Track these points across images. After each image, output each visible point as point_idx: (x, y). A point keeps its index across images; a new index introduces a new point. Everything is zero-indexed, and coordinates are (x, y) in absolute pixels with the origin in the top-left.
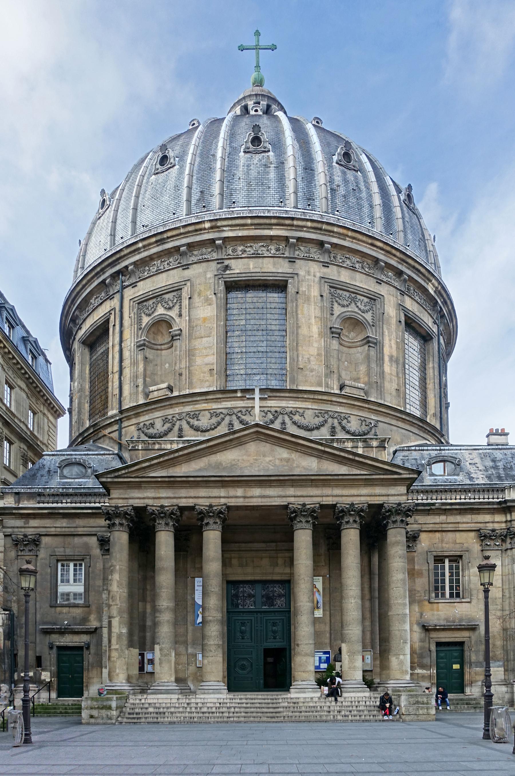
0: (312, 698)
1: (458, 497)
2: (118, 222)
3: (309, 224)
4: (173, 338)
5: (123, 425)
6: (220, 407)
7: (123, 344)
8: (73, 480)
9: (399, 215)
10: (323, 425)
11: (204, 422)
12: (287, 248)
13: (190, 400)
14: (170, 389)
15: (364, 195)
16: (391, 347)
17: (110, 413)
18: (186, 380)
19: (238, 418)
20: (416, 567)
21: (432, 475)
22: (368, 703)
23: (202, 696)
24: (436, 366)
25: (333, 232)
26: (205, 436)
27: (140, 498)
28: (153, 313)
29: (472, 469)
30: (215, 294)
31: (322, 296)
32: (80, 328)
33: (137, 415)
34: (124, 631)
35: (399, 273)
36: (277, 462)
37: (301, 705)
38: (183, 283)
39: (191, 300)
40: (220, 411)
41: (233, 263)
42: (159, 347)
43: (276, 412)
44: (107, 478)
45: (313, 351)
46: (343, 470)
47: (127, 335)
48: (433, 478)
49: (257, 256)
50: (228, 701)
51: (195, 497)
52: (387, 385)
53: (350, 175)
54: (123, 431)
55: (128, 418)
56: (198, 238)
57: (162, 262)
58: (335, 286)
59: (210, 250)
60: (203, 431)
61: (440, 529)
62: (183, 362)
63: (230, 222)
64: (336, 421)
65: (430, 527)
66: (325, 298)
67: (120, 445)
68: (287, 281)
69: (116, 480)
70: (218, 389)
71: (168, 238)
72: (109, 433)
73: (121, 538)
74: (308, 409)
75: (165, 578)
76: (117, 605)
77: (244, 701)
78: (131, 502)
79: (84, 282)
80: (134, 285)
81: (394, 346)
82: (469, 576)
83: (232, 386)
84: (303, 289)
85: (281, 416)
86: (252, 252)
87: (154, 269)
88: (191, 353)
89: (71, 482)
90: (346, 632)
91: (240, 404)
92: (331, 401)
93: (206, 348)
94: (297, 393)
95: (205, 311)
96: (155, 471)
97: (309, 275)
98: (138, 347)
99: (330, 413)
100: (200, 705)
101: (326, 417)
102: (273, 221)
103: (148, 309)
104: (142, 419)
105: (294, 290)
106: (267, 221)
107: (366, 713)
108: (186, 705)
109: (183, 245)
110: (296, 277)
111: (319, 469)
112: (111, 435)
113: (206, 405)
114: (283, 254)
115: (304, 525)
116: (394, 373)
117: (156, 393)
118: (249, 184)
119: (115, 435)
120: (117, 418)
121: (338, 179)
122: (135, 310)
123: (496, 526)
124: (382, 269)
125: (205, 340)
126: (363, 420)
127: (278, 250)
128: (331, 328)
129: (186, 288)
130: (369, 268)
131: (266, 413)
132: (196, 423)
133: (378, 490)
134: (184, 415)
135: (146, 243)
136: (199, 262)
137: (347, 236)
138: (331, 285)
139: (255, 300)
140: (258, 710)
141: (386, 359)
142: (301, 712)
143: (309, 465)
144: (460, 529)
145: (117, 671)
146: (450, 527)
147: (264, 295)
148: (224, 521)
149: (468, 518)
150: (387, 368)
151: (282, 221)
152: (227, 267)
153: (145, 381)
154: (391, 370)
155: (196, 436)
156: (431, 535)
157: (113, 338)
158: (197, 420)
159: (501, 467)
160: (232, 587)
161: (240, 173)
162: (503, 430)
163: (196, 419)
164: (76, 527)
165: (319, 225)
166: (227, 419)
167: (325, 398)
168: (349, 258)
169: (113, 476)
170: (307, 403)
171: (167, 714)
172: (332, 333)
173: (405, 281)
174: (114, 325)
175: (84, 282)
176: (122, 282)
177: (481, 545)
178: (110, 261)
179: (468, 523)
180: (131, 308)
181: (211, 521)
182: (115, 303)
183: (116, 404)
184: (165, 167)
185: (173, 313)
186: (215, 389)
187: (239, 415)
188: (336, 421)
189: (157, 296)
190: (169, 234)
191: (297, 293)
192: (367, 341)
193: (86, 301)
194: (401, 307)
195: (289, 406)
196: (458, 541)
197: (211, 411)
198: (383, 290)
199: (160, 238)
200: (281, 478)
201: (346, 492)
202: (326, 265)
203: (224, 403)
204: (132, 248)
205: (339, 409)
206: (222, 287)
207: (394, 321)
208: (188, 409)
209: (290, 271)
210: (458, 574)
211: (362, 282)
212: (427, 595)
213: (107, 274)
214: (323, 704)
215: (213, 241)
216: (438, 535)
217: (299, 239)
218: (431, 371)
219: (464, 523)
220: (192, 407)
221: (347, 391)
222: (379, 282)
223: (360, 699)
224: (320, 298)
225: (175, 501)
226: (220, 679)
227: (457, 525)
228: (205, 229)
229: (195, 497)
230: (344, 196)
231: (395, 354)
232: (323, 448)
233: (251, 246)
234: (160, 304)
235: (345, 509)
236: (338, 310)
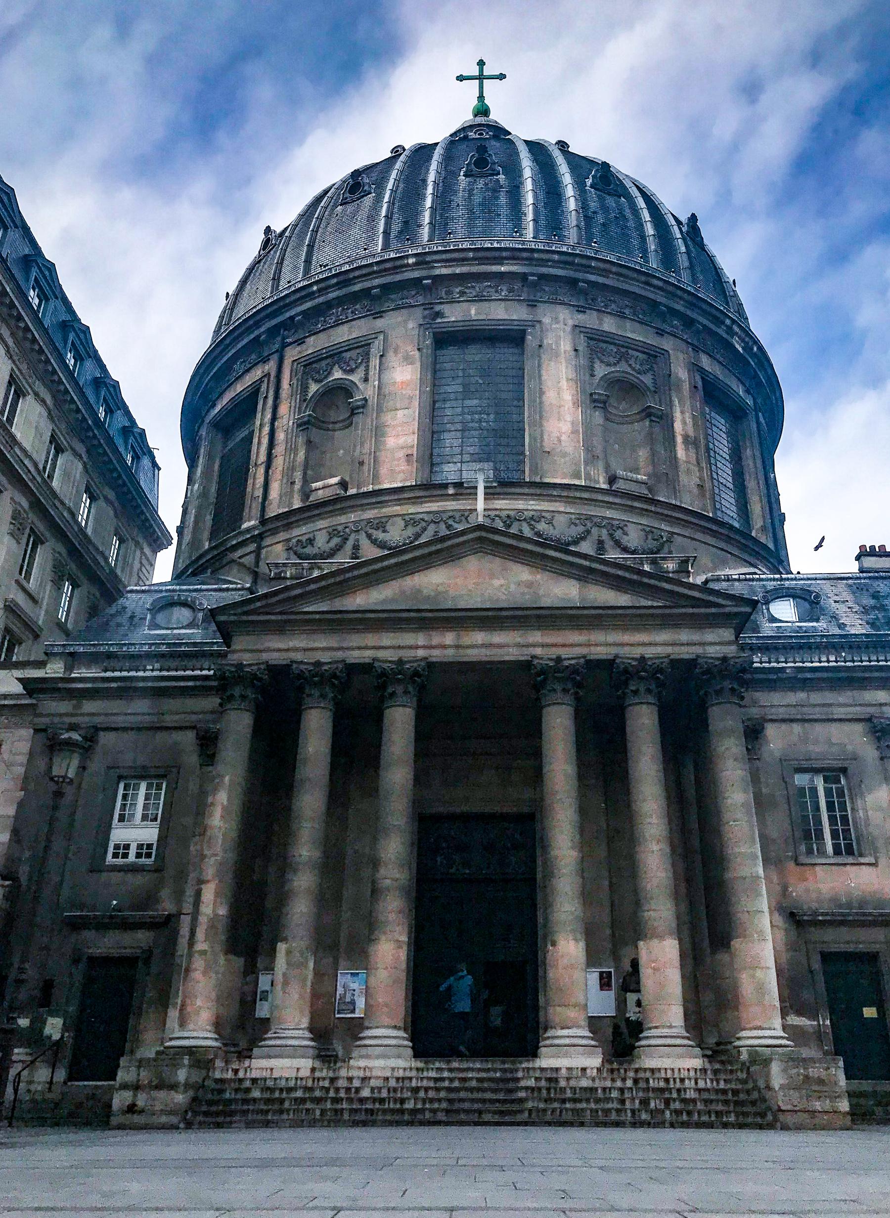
0: (584, 1070)
1: (824, 659)
2: (286, 262)
3: (556, 257)
4: (353, 411)
5: (264, 544)
7: (276, 423)
9: (683, 249)
10: (583, 539)
12: (525, 289)
14: (343, 485)
15: (631, 224)
16: (684, 423)
17: (245, 526)
18: (369, 470)
20: (764, 790)
21: (773, 619)
22: (701, 1084)
23: (362, 1063)
24: (758, 454)
25: (590, 266)
27: (279, 650)
28: (326, 377)
29: (841, 609)
30: (419, 349)
31: (576, 350)
32: (214, 406)
33: (288, 526)
34: (223, 911)
35: (689, 323)
36: (513, 587)
37: (563, 1083)
38: (374, 336)
39: (384, 359)
41: (446, 309)
42: (331, 426)
43: (508, 516)
44: (230, 615)
45: (565, 427)
46: (623, 599)
47: (283, 409)
48: (774, 625)
49: (480, 299)
50: (414, 1074)
51: (374, 648)
52: (683, 478)
53: (610, 201)
54: (264, 551)
55: (274, 532)
56: (398, 278)
57: (343, 309)
59: (413, 293)
61: (799, 717)
62: (367, 446)
63: (444, 256)
65: (782, 713)
66: (581, 353)
67: (256, 576)
68: (524, 331)
69: (245, 618)
70: (419, 483)
71: (355, 278)
72: (240, 558)
73: (239, 725)
75: (310, 803)
76: (216, 855)
77: (446, 1074)
78: (265, 656)
79: (227, 341)
80: (300, 342)
81: (689, 420)
82: (866, 810)
83: (438, 479)
85: (516, 524)
86: (474, 294)
87: (331, 321)
88: (379, 432)
89: (167, 635)
90: (646, 914)
91: (451, 505)
92: (596, 500)
94: (543, 489)
95: (402, 374)
96: (310, 603)
97: (557, 323)
98: (299, 426)
99: (595, 520)
100: (356, 1083)
101: (589, 525)
102: (504, 254)
103: (319, 372)
104: (296, 532)
106: (497, 254)
107: (700, 1106)
108: (326, 1084)
110: (538, 326)
111: (583, 600)
112: (242, 560)
114: (519, 296)
115: (559, 696)
116: (693, 460)
117: (320, 492)
118: (471, 211)
119: (249, 560)
120: (256, 532)
121: (593, 205)
122: (299, 376)
124: (662, 316)
125: (400, 413)
126: (648, 532)
127: (511, 291)
128: (591, 395)
129: (377, 342)
130: (644, 314)
133: (685, 636)
135: (322, 285)
137: (611, 272)
138: (591, 336)
140: (476, 1095)
141: (679, 439)
142: (564, 1101)
143: (564, 591)
145: (199, 1003)
146: (817, 713)
148: (422, 688)
150: (681, 453)
151: (518, 254)
152: (439, 314)
153: (305, 474)
154: (687, 455)
156: (784, 726)
157: (263, 417)
160: (428, 829)
161: (459, 198)
162: (882, 547)
163: (381, 529)
165: (570, 259)
167: (586, 495)
168: (615, 302)
169: (239, 611)
170: (557, 504)
171: (287, 1105)
172: (595, 401)
173: (698, 332)
174: (266, 397)
175: (227, 341)
176: (284, 339)
177: (878, 748)
178: (270, 310)
180: (294, 374)
181: (400, 689)
182: (271, 366)
183: (256, 511)
184: (357, 196)
185: (355, 378)
188: (604, 531)
189: (335, 356)
190: (357, 273)
191: (540, 346)
192: (648, 413)
193: (228, 367)
194: (695, 368)
195: (530, 508)
198: (667, 344)
199: (344, 279)
200: (520, 613)
201: (627, 638)
203: (426, 505)
204: (304, 294)
205: (609, 513)
207: (686, 386)
209: (530, 317)
210: (843, 808)
211: (634, 332)
212: (792, 848)
213: (262, 329)
214: (608, 1084)
215: (419, 280)
216: (797, 728)
217: (542, 277)
218: (751, 463)
221: (620, 485)
222: (660, 333)
223: (684, 1074)
225: (339, 655)
226: (402, 1025)
228: (408, 265)
229: (374, 648)
230: (604, 225)
231: (691, 433)
232: (587, 563)
233: (473, 287)
234: (337, 366)
235: (631, 669)
236: (601, 370)
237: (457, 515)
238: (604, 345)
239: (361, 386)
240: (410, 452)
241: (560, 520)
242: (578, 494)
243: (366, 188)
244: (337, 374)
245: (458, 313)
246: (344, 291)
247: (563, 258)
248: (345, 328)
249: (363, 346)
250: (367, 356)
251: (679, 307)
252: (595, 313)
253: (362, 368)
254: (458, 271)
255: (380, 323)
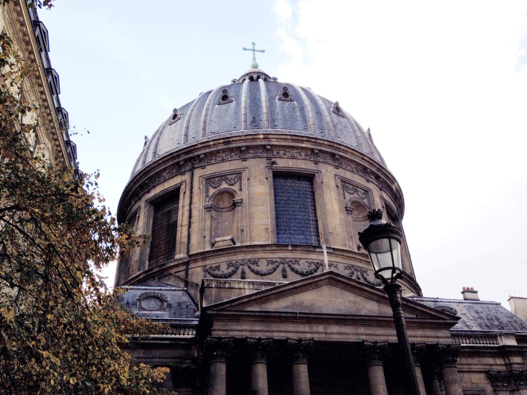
1: (464, 342)
6: (275, 256)
8: (150, 312)
11: (263, 267)
13: (252, 250)
18: (247, 234)
19: (290, 266)
25: (340, 149)
26: (264, 279)
30: (267, 178)
31: (337, 186)
39: (249, 181)
40: (274, 260)
41: (278, 161)
43: (318, 263)
49: (293, 158)
56: (254, 143)
58: (345, 182)
59: (261, 151)
60: (262, 275)
64: (359, 273)
68: (315, 175)
70: (273, 243)
71: (233, 141)
74: (339, 262)
84: (325, 181)
86: (290, 155)
88: (250, 216)
93: (261, 214)
101: (353, 269)
105: (320, 181)
109: (243, 147)
113: (263, 254)
123: (500, 368)
125: (260, 208)
127: (306, 155)
131: (311, 264)
132: (256, 268)
134: (246, 261)
136: (254, 157)
139: (293, 185)
144: (473, 370)
147: (298, 182)
149: (476, 360)
152: (274, 163)
155: (256, 279)
158: (257, 266)
159: (485, 318)
164: (153, 358)
166: (281, 266)
167: (350, 255)
170: (338, 258)
179: (477, 365)
186: (271, 243)
187: (290, 264)
190: (234, 139)
196: (474, 381)
197: (268, 260)
202: (337, 167)
206: (271, 175)
208: (249, 256)
209: (316, 169)
215: (265, 146)
219: (474, 365)
220: (252, 255)
224: (336, 187)
227: (470, 366)
237: (293, 260)
238: (348, 185)
239: (239, 192)
240: (267, 227)
241: (340, 266)
242: (347, 255)
243: (230, 99)
244: (224, 186)
245: (284, 163)
246: (227, 146)
247: (330, 144)
248: (228, 163)
249: (238, 174)
250: (240, 179)
251: (374, 170)
252: (342, 170)
253: (238, 184)
254: (283, 144)
255: (245, 164)
